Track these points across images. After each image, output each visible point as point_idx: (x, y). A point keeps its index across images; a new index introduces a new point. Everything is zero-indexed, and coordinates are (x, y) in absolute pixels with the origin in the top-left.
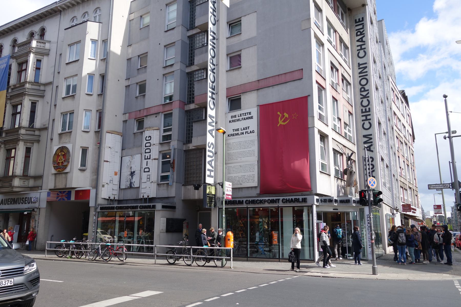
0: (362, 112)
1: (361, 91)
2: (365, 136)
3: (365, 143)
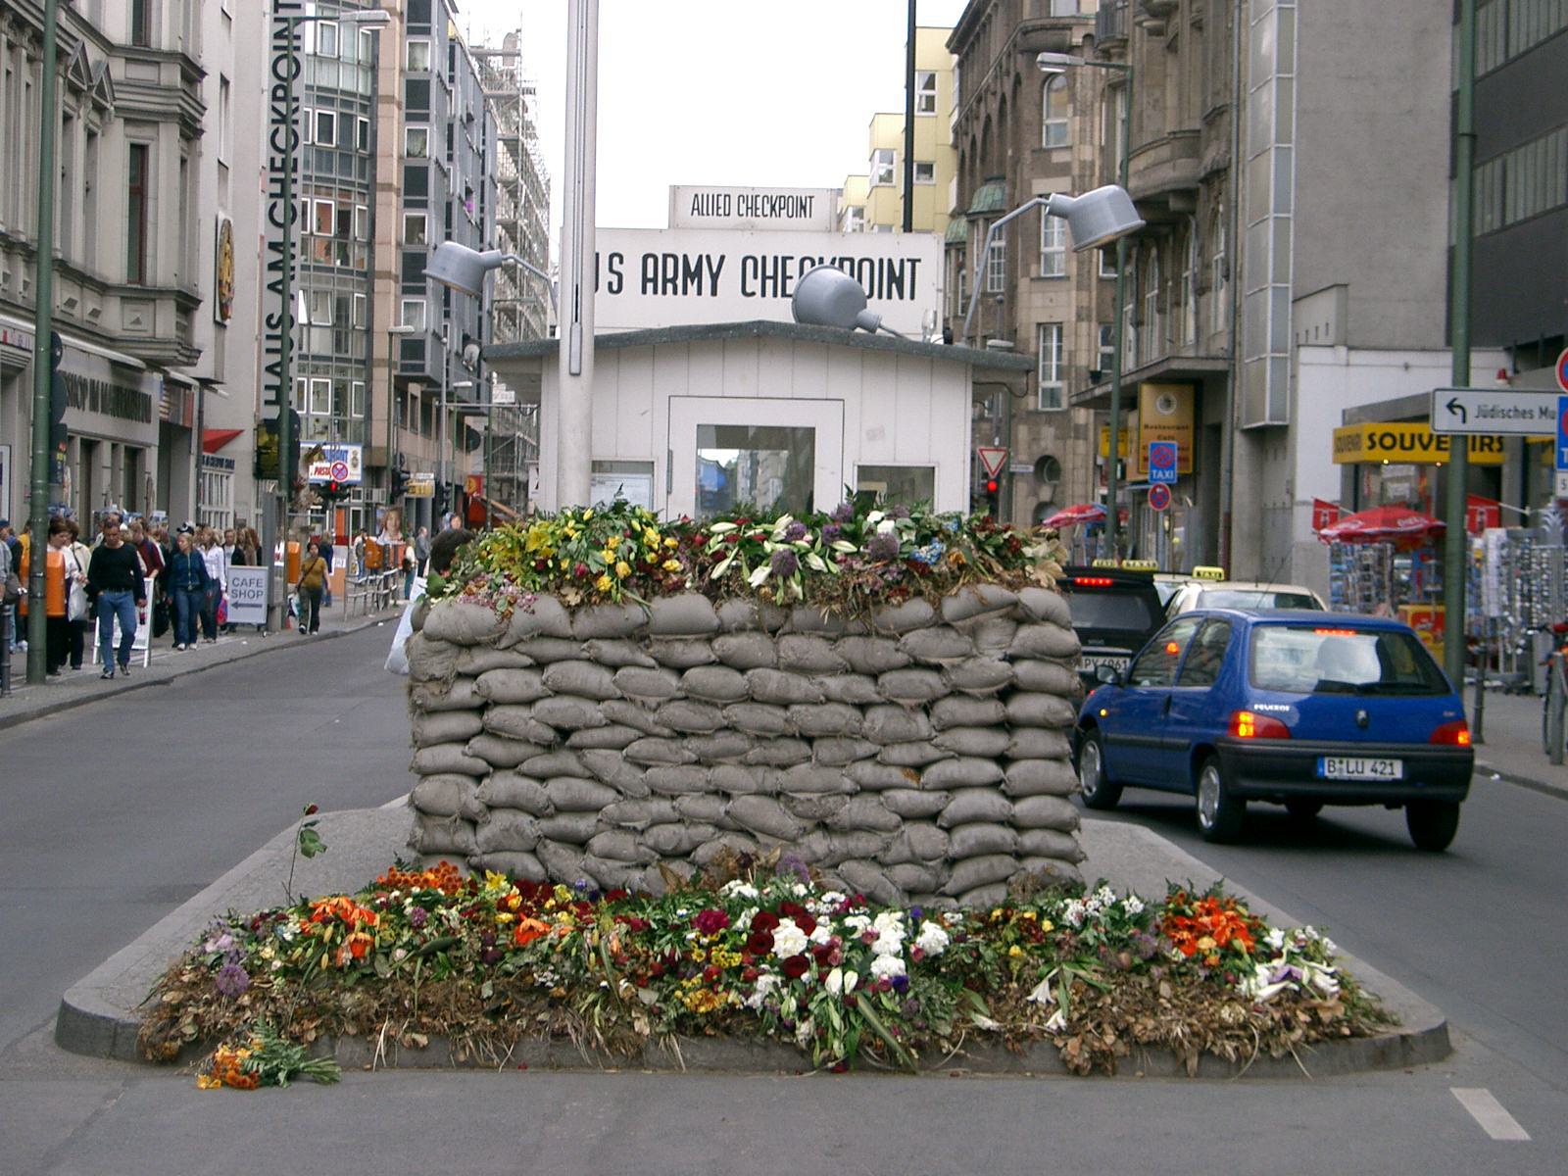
0: (273, 169)
1: (275, 98)
2: (273, 246)
3: (273, 267)
